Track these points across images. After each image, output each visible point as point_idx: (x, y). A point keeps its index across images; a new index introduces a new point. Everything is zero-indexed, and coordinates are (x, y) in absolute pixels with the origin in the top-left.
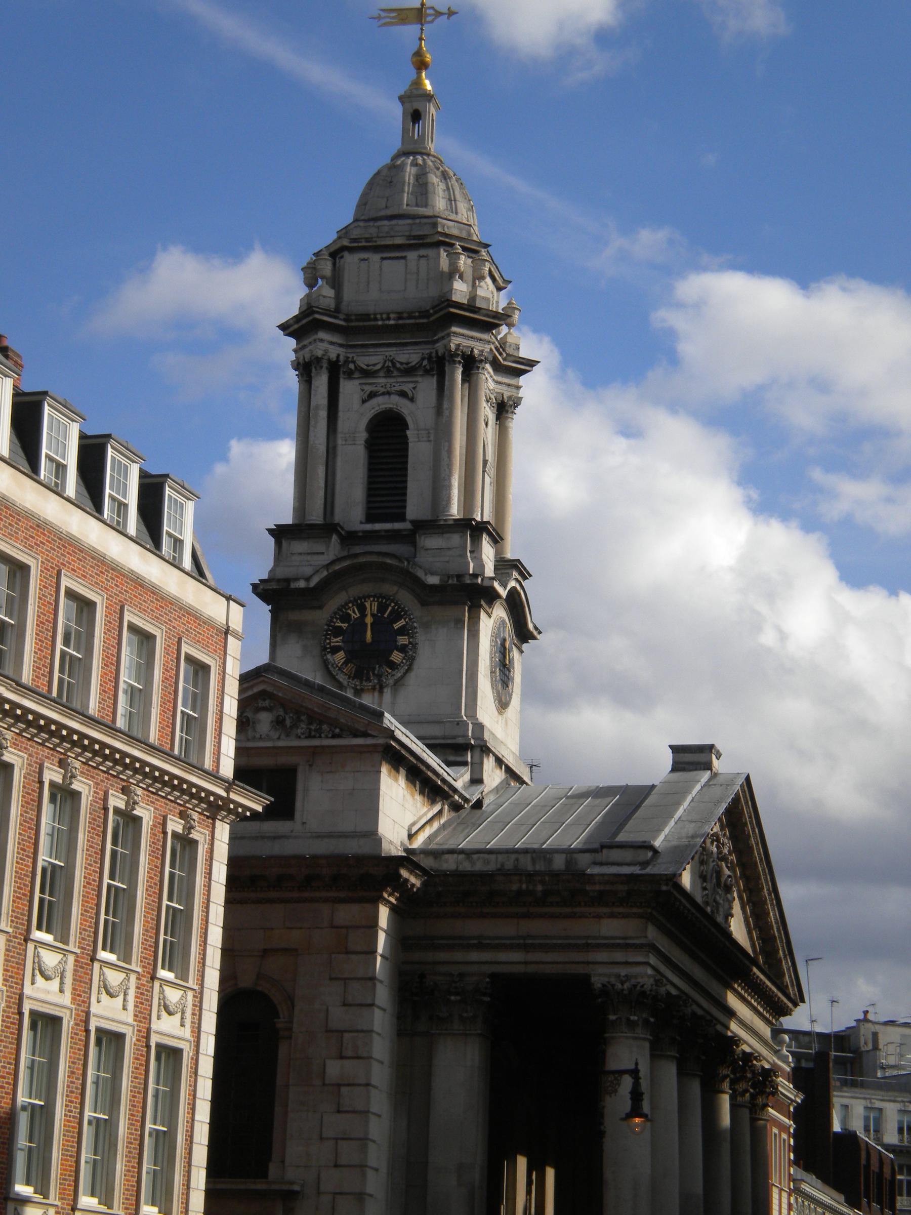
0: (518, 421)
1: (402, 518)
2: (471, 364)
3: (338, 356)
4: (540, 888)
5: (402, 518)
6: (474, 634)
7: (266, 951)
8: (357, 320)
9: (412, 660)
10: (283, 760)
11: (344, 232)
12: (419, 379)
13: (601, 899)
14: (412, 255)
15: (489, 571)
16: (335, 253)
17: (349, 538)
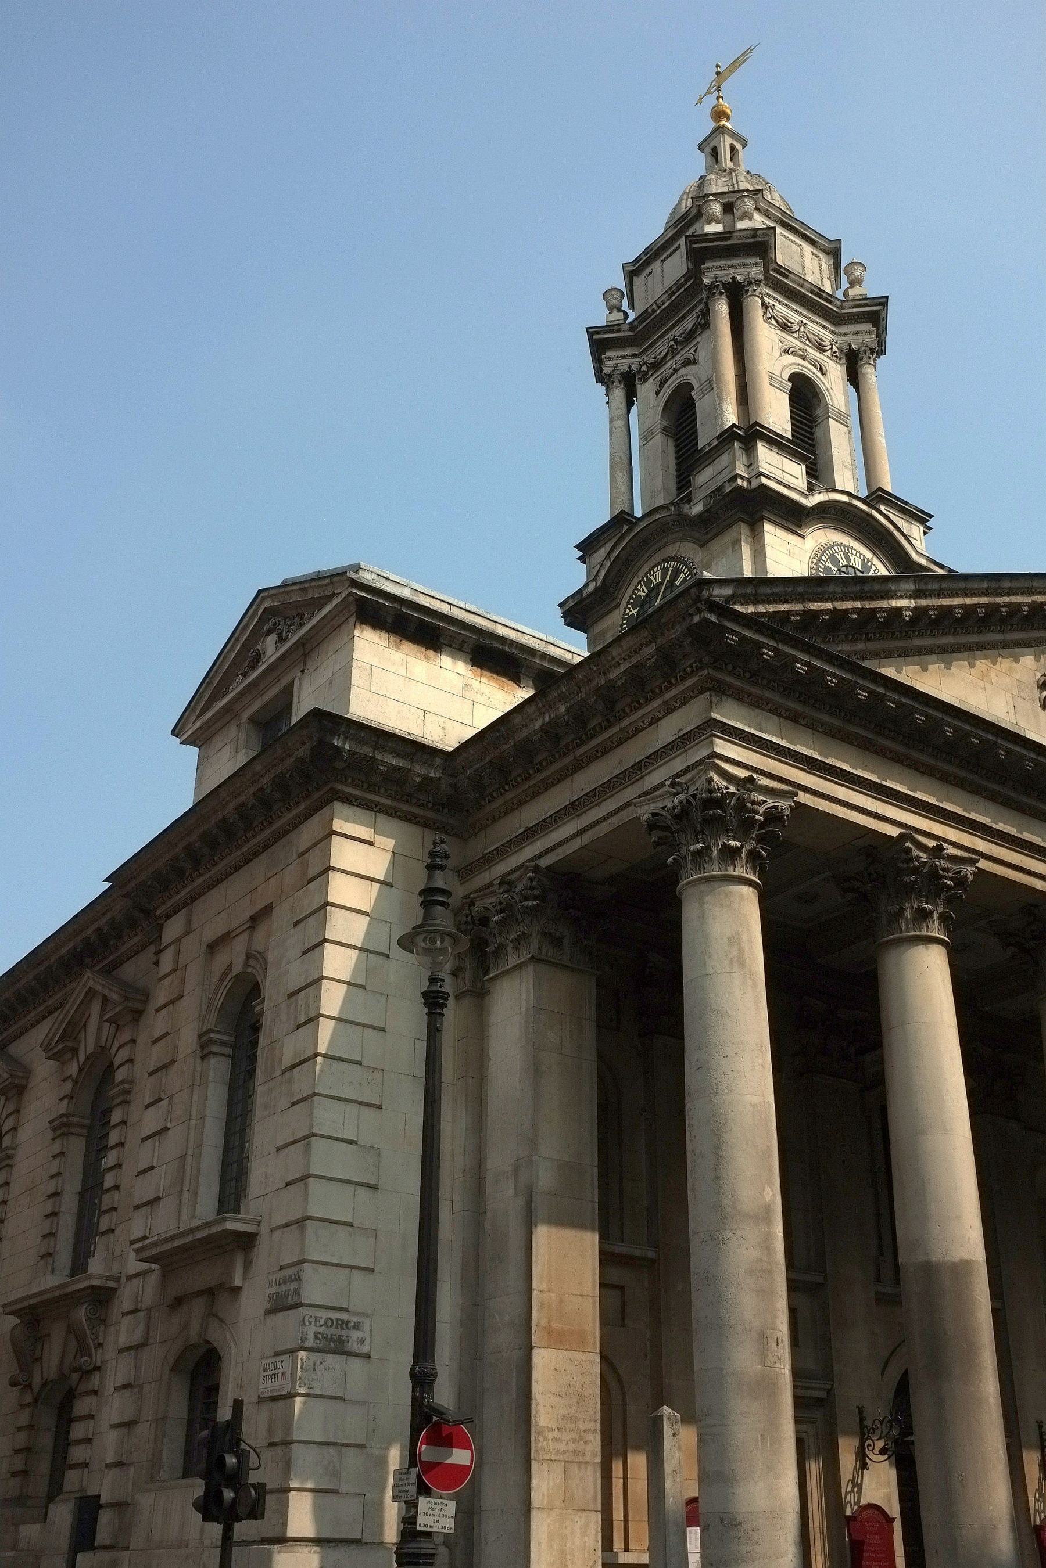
3: (630, 367)
8: (640, 323)
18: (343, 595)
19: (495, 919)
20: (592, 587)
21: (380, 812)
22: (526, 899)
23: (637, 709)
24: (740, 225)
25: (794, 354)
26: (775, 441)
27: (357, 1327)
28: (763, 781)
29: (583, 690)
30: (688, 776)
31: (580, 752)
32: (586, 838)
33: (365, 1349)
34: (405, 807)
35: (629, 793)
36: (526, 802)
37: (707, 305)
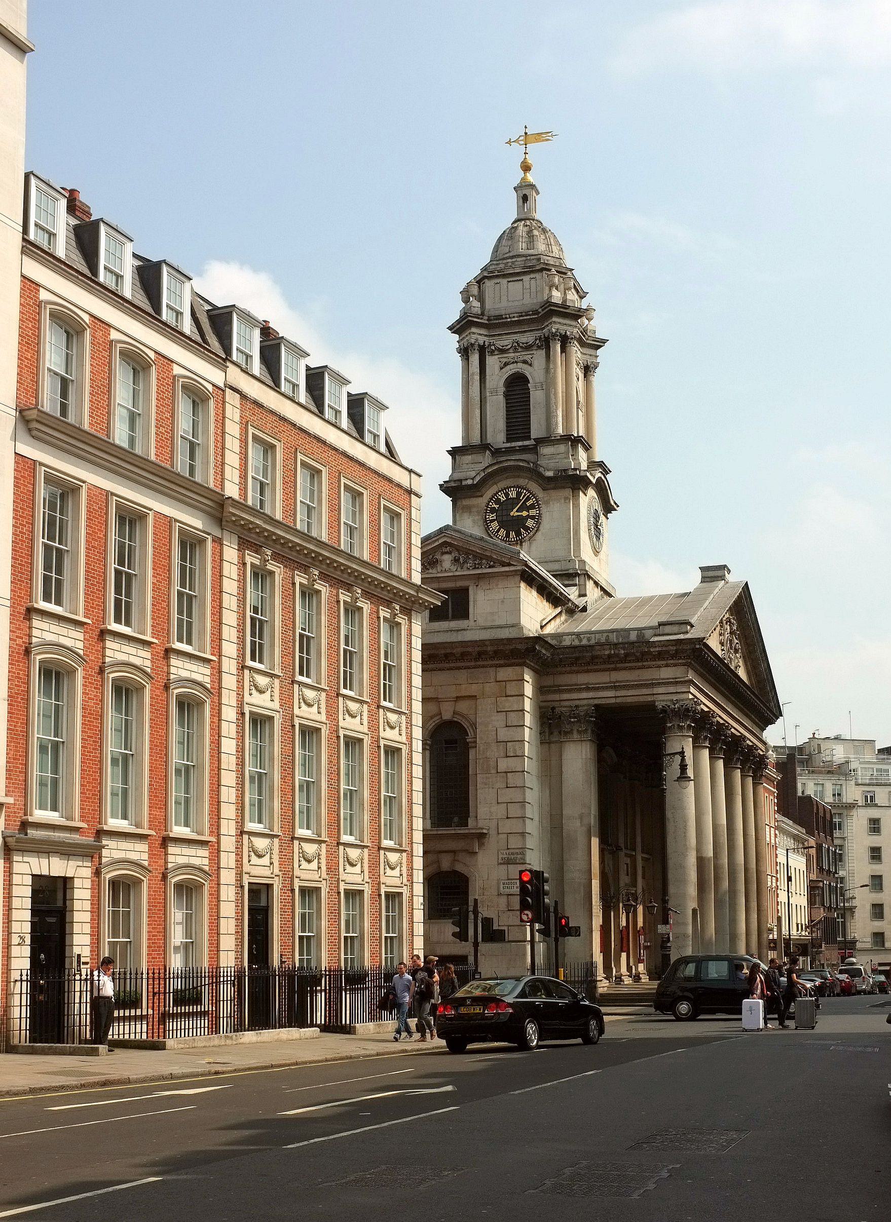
0: (597, 378)
1: (528, 438)
2: (565, 341)
5: (529, 438)
6: (577, 506)
7: (457, 697)
8: (494, 319)
9: (538, 523)
10: (460, 584)
11: (484, 269)
12: (534, 352)
13: (660, 656)
14: (526, 278)
15: (584, 466)
16: (480, 281)
17: (496, 452)
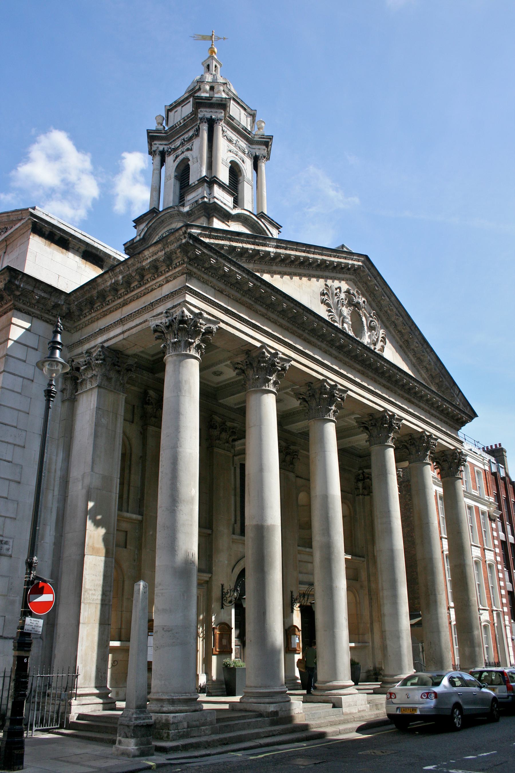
3: (164, 149)
4: (120, 277)
8: (170, 131)
18: (26, 219)
19: (82, 368)
20: (138, 238)
21: (34, 317)
22: (97, 360)
23: (153, 280)
24: (216, 96)
25: (233, 152)
26: (221, 186)
27: (6, 543)
28: (205, 315)
29: (130, 269)
30: (174, 310)
31: (126, 297)
32: (126, 335)
33: (10, 553)
34: (46, 316)
35: (146, 316)
36: (101, 318)
37: (199, 126)
